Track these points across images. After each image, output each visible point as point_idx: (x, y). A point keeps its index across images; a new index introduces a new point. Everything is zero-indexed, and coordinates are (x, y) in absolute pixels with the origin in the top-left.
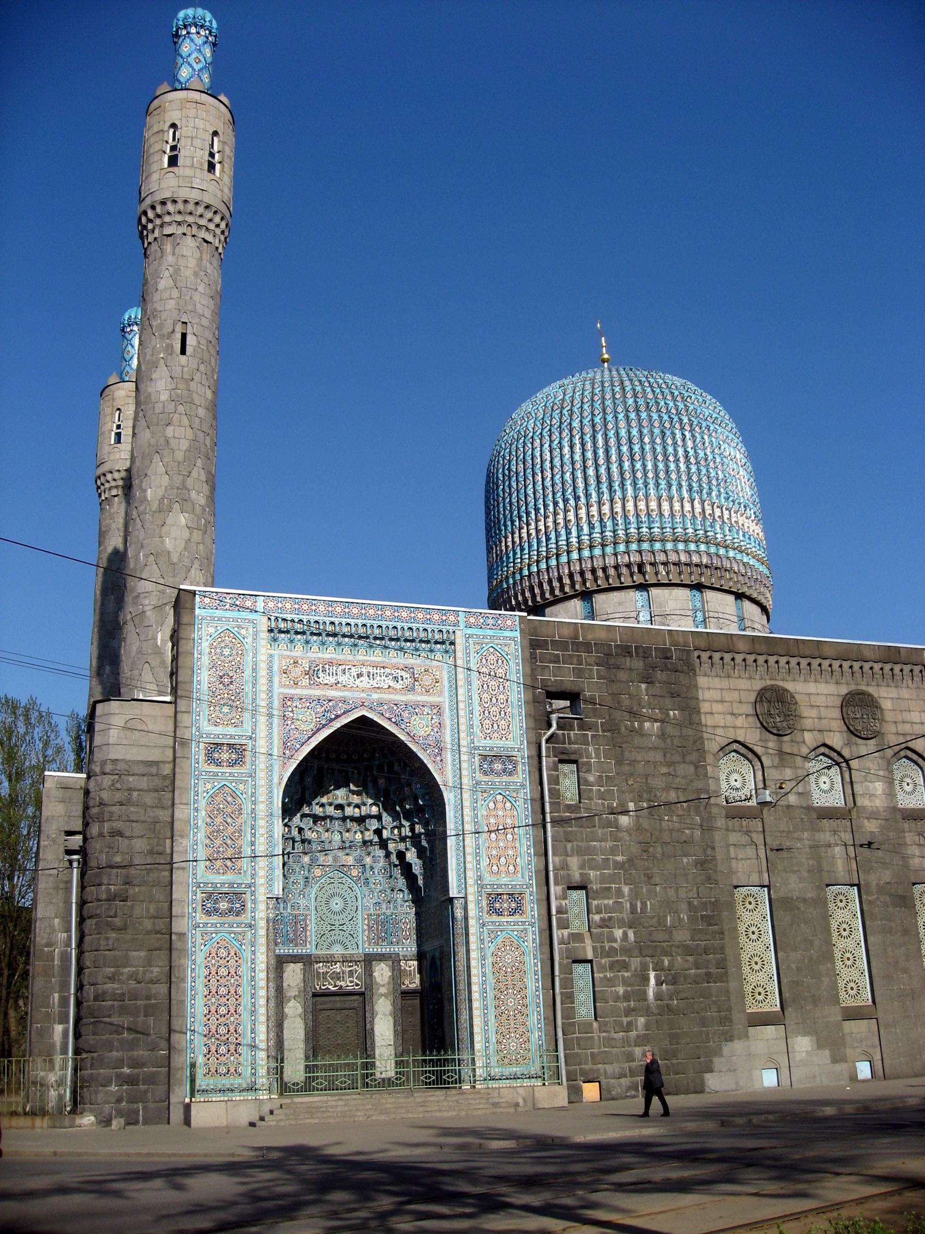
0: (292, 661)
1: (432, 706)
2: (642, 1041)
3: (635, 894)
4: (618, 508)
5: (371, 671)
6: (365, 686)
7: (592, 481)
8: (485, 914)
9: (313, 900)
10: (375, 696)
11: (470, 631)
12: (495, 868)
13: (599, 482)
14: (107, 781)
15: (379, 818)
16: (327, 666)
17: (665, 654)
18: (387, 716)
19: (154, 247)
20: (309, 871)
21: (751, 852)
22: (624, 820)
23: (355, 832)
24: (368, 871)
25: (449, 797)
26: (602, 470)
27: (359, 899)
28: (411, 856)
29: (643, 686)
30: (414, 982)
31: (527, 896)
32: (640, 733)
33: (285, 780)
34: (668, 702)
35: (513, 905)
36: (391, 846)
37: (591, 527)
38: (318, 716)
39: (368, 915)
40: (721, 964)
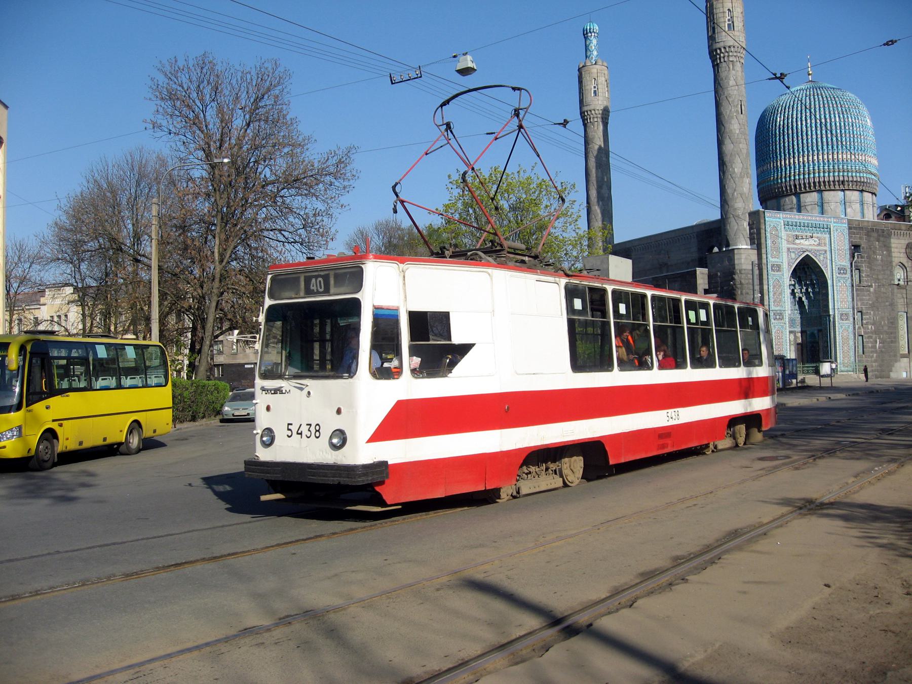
2: (876, 361)
3: (874, 314)
4: (835, 157)
6: (809, 245)
7: (825, 143)
13: (828, 144)
14: (743, 276)
15: (794, 285)
17: (883, 231)
19: (724, 65)
21: (902, 300)
22: (872, 290)
25: (829, 282)
26: (829, 140)
28: (804, 299)
30: (800, 341)
32: (876, 259)
37: (824, 164)
40: (895, 338)
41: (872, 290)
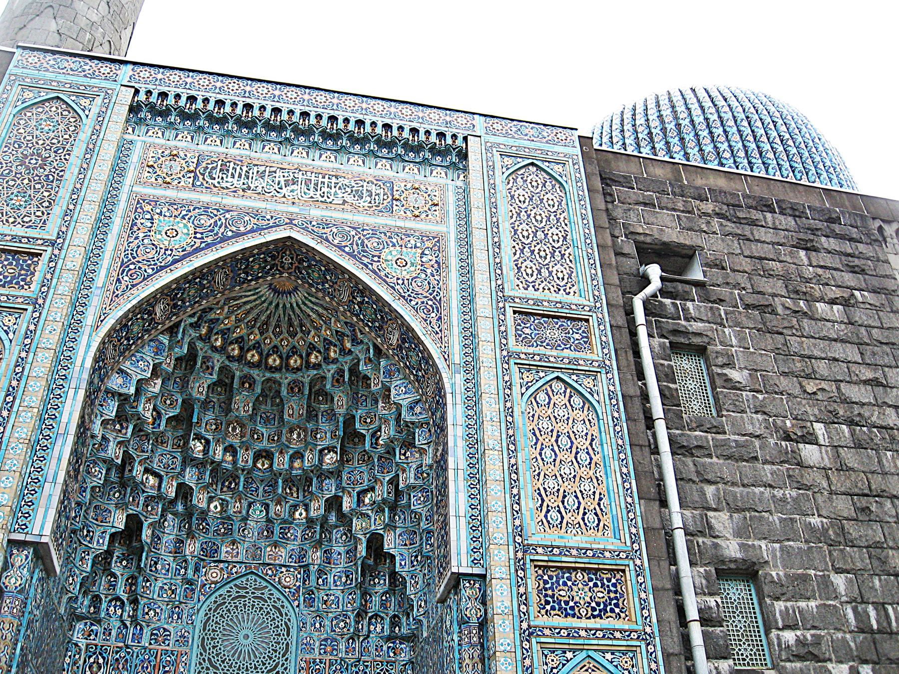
0: (167, 152)
1: (424, 237)
5: (313, 178)
8: (533, 609)
9: (199, 625)
10: (316, 213)
11: (493, 139)
12: (553, 514)
15: (336, 474)
16: (232, 165)
18: (336, 242)
20: (197, 570)
22: (810, 453)
23: (295, 507)
24: (313, 577)
25: (453, 383)
27: (294, 632)
29: (802, 253)
31: (630, 574)
33: (110, 322)
34: (848, 278)
35: (601, 595)
36: (357, 524)
38: (198, 230)
39: (307, 662)
41: (810, 453)
